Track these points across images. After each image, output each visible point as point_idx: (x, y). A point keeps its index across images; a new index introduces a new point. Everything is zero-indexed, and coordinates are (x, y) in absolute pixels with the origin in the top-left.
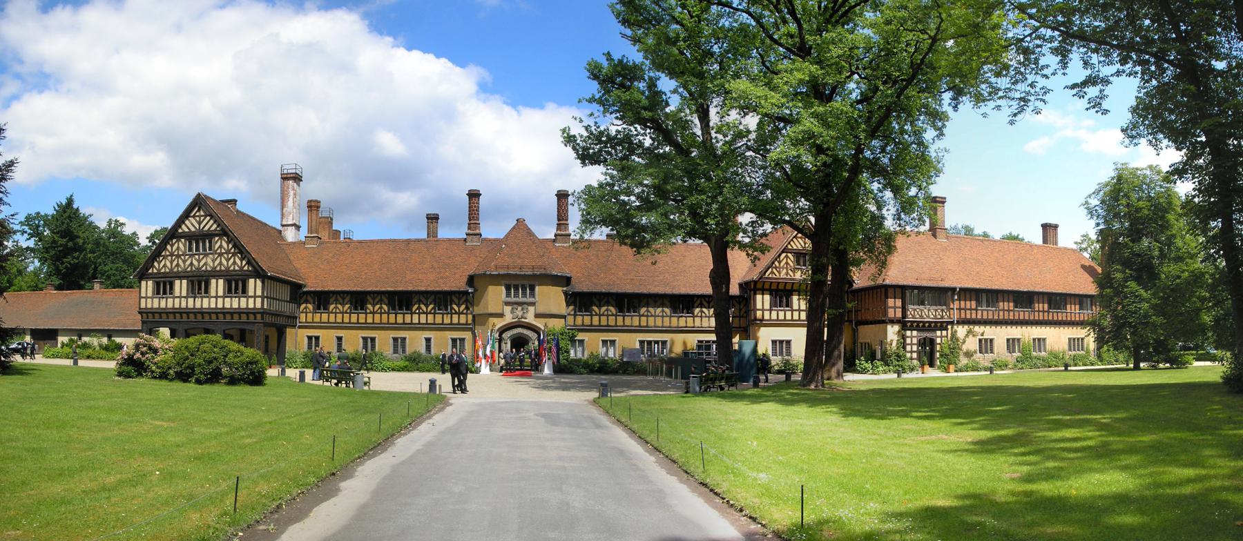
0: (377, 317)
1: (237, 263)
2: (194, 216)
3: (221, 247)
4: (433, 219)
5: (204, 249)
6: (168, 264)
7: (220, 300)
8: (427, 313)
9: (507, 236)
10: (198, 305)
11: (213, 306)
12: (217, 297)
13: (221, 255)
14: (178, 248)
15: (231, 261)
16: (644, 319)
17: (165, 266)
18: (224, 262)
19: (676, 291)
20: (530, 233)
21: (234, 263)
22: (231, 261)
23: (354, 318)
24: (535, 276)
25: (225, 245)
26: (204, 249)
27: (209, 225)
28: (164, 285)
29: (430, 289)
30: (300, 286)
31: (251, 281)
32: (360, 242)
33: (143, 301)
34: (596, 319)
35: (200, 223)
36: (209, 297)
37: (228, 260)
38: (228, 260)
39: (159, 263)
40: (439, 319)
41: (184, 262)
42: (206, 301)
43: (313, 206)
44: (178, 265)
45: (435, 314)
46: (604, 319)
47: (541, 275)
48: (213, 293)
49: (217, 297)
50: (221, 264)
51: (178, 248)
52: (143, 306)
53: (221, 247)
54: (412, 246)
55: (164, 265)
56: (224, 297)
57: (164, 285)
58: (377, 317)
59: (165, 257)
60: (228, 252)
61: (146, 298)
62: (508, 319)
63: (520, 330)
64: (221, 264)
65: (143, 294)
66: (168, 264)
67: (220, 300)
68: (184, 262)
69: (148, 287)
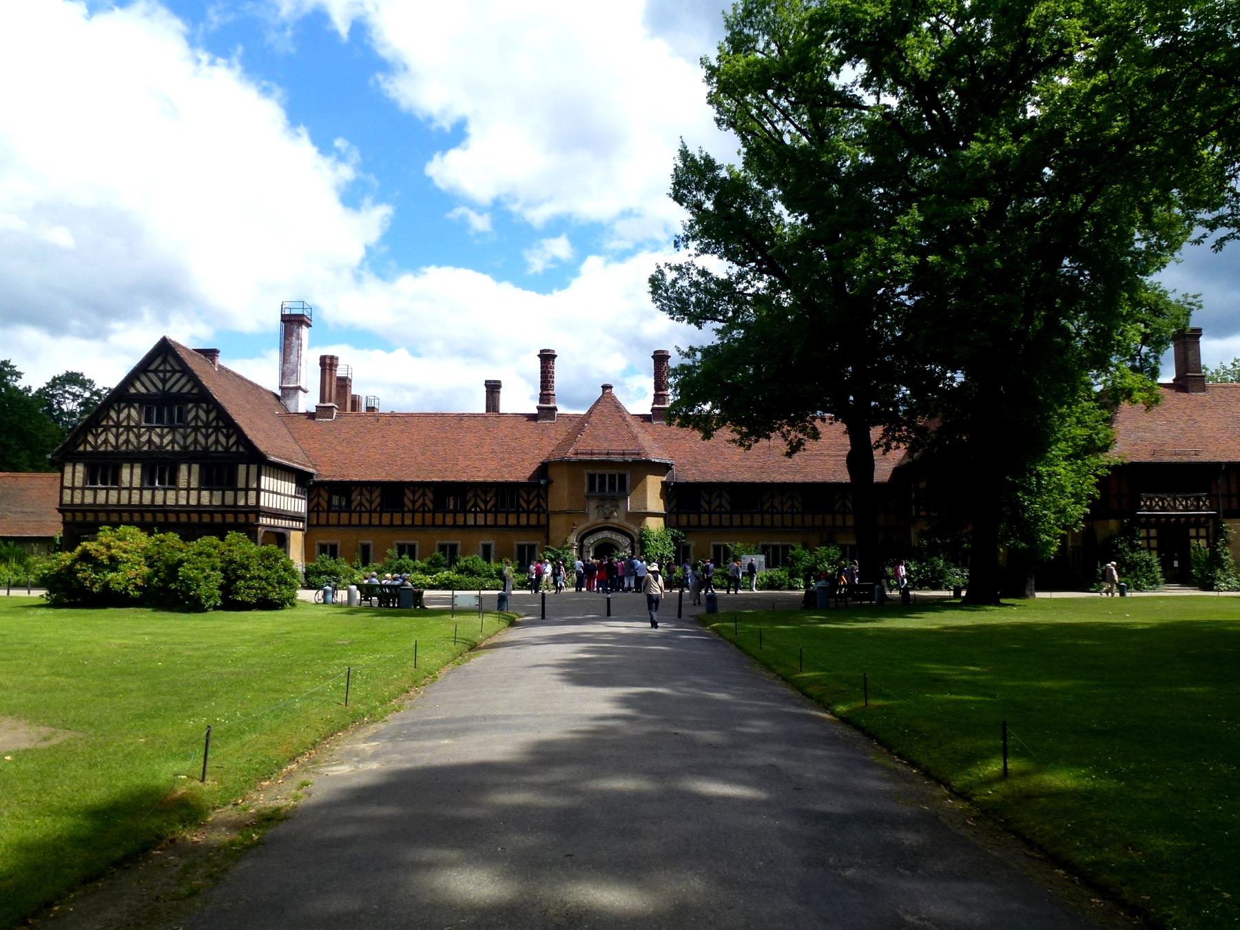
0: (418, 517)
1: (218, 442)
2: (156, 371)
3: (197, 417)
4: (493, 388)
5: (171, 420)
6: (112, 439)
7: (194, 494)
8: (486, 512)
9: (590, 412)
10: (159, 500)
11: (183, 502)
12: (188, 489)
13: (196, 429)
14: (129, 417)
15: (212, 438)
16: (767, 517)
17: (106, 441)
18: (201, 439)
19: (809, 479)
20: (618, 407)
21: (217, 442)
22: (212, 438)
23: (386, 519)
24: (625, 463)
25: (202, 415)
26: (171, 420)
27: (178, 385)
28: (104, 469)
29: (489, 480)
30: (310, 475)
31: (242, 469)
32: (393, 415)
33: (67, 493)
34: (705, 518)
35: (164, 381)
36: (178, 490)
37: (207, 437)
38: (207, 437)
39: (96, 436)
40: (501, 520)
41: (138, 436)
42: (171, 495)
43: (328, 364)
44: (127, 441)
45: (496, 513)
46: (715, 518)
47: (634, 462)
48: (182, 482)
49: (188, 489)
50: (196, 441)
51: (129, 417)
52: (67, 499)
53: (197, 417)
54: (466, 423)
55: (105, 440)
56: (199, 490)
57: (104, 469)
58: (418, 517)
59: (107, 429)
60: (207, 425)
61: (73, 488)
62: (594, 518)
63: (607, 534)
64: (196, 441)
65: (67, 483)
66: (112, 439)
67: (194, 494)
68: (138, 436)
69: (76, 474)
